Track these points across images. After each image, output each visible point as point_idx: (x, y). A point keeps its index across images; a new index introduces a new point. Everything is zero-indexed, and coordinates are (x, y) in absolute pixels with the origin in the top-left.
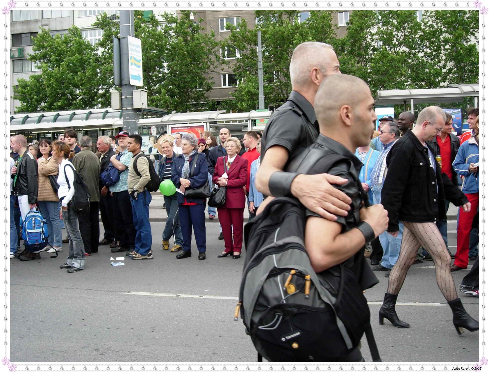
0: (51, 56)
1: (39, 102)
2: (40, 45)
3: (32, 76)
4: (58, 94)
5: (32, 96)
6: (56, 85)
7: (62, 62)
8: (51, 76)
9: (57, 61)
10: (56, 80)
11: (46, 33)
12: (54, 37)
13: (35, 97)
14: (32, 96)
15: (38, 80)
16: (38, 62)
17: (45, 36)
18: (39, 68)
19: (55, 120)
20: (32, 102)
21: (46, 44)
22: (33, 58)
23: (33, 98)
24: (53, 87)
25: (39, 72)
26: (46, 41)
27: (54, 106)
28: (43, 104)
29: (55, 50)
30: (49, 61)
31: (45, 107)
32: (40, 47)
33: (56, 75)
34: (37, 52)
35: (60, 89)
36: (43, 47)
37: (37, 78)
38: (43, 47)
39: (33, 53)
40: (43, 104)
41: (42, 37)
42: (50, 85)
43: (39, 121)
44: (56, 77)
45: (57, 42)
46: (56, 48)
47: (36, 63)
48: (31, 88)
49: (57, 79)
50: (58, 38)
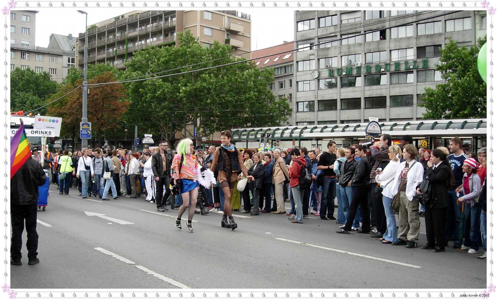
0: (457, 67)
2: (447, 56)
3: (439, 86)
4: (464, 102)
5: (438, 103)
7: (468, 72)
8: (459, 86)
9: (463, 71)
11: (455, 44)
12: (459, 48)
13: (441, 104)
14: (438, 103)
15: (444, 89)
16: (444, 72)
18: (446, 78)
19: (463, 127)
21: (453, 56)
22: (440, 68)
23: (438, 105)
24: (459, 96)
25: (444, 82)
26: (452, 53)
28: (447, 112)
30: (454, 71)
31: (450, 114)
32: (447, 58)
33: (463, 84)
34: (443, 63)
36: (450, 58)
37: (443, 87)
38: (450, 58)
39: (440, 63)
40: (447, 112)
41: (449, 49)
42: (457, 93)
43: (447, 127)
45: (464, 53)
46: (463, 60)
47: (442, 73)
48: (438, 96)
49: (463, 88)
50: (464, 49)
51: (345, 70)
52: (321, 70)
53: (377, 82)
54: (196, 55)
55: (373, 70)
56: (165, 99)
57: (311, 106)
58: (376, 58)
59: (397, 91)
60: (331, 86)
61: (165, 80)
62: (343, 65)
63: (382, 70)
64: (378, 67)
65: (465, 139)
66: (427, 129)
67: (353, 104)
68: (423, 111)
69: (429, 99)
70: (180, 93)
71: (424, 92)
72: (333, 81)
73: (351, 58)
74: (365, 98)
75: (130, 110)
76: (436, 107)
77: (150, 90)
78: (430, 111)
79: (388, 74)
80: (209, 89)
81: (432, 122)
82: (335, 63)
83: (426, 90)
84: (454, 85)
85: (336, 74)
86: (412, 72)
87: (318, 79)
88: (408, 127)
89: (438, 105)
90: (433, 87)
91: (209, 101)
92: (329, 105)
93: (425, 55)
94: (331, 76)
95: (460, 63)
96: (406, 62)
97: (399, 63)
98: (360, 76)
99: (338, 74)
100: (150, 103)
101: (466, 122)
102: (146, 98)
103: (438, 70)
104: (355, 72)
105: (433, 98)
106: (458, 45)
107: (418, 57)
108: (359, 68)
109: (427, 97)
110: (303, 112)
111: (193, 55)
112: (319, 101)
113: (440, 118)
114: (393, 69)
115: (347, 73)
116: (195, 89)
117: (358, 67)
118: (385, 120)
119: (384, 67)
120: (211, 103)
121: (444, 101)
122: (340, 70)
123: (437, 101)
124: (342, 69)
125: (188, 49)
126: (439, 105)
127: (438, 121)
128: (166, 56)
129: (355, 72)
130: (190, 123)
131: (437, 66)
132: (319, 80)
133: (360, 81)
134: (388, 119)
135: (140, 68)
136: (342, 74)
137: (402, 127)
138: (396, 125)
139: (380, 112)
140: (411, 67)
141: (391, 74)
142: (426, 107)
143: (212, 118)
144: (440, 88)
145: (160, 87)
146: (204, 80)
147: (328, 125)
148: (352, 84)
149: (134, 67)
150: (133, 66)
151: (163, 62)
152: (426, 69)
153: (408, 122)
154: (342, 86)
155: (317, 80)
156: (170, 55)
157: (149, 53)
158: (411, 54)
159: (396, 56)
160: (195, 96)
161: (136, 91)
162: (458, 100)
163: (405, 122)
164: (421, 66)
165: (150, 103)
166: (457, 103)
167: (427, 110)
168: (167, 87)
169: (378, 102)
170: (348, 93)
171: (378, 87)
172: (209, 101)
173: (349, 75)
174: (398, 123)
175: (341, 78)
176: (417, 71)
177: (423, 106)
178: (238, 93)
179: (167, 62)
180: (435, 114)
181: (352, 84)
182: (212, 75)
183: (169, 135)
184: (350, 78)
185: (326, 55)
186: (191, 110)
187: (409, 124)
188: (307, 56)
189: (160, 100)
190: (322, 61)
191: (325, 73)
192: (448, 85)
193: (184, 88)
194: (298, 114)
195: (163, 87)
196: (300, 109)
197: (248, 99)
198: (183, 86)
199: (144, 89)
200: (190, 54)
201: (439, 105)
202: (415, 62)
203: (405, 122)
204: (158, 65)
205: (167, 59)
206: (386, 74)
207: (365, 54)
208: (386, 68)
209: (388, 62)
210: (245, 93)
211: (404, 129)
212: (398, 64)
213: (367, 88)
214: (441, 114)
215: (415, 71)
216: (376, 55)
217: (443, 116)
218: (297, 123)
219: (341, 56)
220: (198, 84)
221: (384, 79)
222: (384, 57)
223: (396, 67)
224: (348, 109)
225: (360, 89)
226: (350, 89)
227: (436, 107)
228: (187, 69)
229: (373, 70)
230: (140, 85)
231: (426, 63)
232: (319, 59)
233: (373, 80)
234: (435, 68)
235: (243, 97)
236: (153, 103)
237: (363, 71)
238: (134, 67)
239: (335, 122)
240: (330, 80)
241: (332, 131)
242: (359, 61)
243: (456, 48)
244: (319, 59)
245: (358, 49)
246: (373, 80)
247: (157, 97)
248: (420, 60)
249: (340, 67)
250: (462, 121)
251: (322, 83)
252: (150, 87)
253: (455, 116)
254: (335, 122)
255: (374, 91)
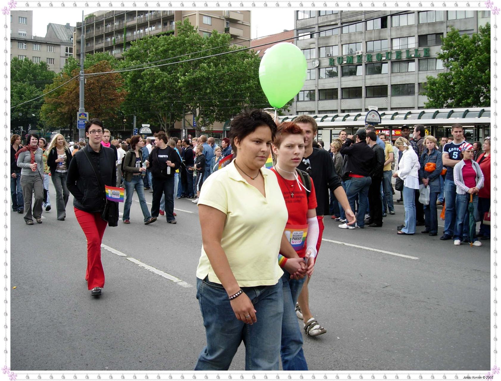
0: (459, 55)
1: (446, 98)
3: (441, 75)
4: (466, 91)
5: (440, 92)
6: (465, 83)
8: (461, 74)
9: (465, 60)
10: (466, 78)
11: (457, 32)
12: (461, 37)
13: (443, 93)
14: (440, 92)
15: (446, 78)
16: (446, 60)
17: (454, 36)
18: (448, 67)
20: (439, 98)
21: (454, 44)
22: (442, 57)
23: (440, 94)
24: (461, 84)
25: (445, 70)
26: (454, 41)
27: (462, 103)
28: (449, 101)
29: (463, 48)
30: (456, 60)
31: (452, 103)
32: (449, 47)
33: (466, 72)
34: (445, 51)
35: (468, 87)
36: (451, 46)
37: (445, 75)
38: (451, 46)
39: (442, 52)
40: (449, 101)
41: (451, 37)
42: (459, 82)
43: (449, 116)
44: (466, 75)
45: (466, 42)
46: (465, 48)
47: (444, 61)
50: (466, 37)
51: (346, 59)
52: (321, 59)
53: (379, 71)
54: (195, 44)
55: (375, 59)
56: (164, 89)
57: (311, 95)
58: (376, 47)
59: (398, 80)
60: (332, 74)
61: (163, 69)
62: (344, 54)
63: (384, 58)
64: (379, 56)
65: (467, 128)
66: (429, 118)
67: (354, 93)
68: (425, 100)
69: (430, 88)
70: (178, 82)
71: (426, 81)
72: (334, 70)
73: (352, 46)
74: (366, 87)
75: (128, 99)
76: (438, 95)
77: (148, 80)
78: (432, 100)
79: (389, 62)
80: (208, 79)
81: (434, 110)
82: (336, 52)
83: (428, 79)
84: (456, 74)
85: (336, 63)
86: (413, 61)
87: (319, 68)
88: (409, 116)
89: (440, 94)
90: (435, 76)
91: (208, 91)
92: (330, 94)
93: (427, 43)
94: (332, 64)
95: (462, 52)
96: (408, 51)
97: (400, 51)
98: (361, 65)
99: (339, 62)
100: (149, 93)
101: (468, 111)
102: (144, 88)
103: (440, 58)
104: (356, 61)
105: (435, 87)
106: (460, 33)
107: (420, 45)
108: (360, 57)
109: (429, 85)
110: (304, 101)
111: (192, 44)
112: (319, 90)
113: (442, 107)
114: (394, 57)
115: (347, 61)
116: (194, 79)
117: (359, 56)
118: (386, 109)
119: (386, 55)
120: (210, 93)
121: (446, 89)
122: (340, 59)
123: (439, 90)
124: (342, 58)
125: (187, 39)
126: (440, 94)
127: (440, 110)
128: (164, 45)
129: (356, 61)
130: (189, 113)
131: (439, 54)
132: (319, 69)
133: (361, 70)
134: (389, 108)
135: (138, 58)
136: (342, 62)
137: (404, 116)
138: (397, 114)
139: (381, 102)
140: (413, 56)
141: (392, 63)
142: (428, 96)
143: (211, 108)
144: (442, 77)
145: (159, 76)
146: (204, 69)
147: (328, 115)
148: (353, 73)
149: (132, 56)
150: (130, 55)
151: (161, 51)
152: (428, 57)
153: (409, 111)
154: (343, 75)
155: (317, 69)
156: (168, 44)
157: (146, 42)
158: (413, 43)
159: (397, 45)
160: (194, 85)
161: (134, 80)
162: (461, 89)
163: (406, 111)
164: (422, 54)
165: (149, 93)
166: (458, 91)
167: (428, 99)
168: (166, 77)
169: (379, 91)
170: (349, 82)
171: (380, 75)
172: (208, 91)
173: (350, 63)
174: (399, 112)
175: (342, 67)
176: (419, 60)
177: (424, 94)
178: (237, 83)
179: (166, 51)
180: (437, 102)
181: (353, 73)
182: (212, 64)
183: (168, 125)
184: (350, 67)
185: (327, 44)
186: (191, 100)
187: (410, 113)
188: (307, 44)
189: (159, 89)
190: (323, 50)
191: (326, 62)
192: (450, 74)
193: (182, 78)
194: (299, 103)
195: (162, 76)
196: (301, 98)
197: (248, 88)
198: (181, 75)
199: (142, 79)
200: (188, 43)
201: (440, 94)
202: (417, 50)
203: (406, 111)
204: (157, 54)
205: (165, 48)
206: (387, 63)
207: (366, 42)
208: (387, 57)
209: (389, 51)
210: (244, 82)
211: (406, 118)
212: (399, 53)
213: (369, 76)
214: (444, 103)
215: (416, 60)
216: (377, 43)
217: (445, 105)
218: (297, 112)
219: (342, 45)
220: (197, 74)
221: (386, 68)
222: (385, 45)
223: (397, 56)
224: (349, 98)
225: (361, 78)
226: (351, 78)
227: (438, 95)
228: (186, 58)
229: (375, 59)
230: (138, 75)
231: (427, 51)
232: (319, 48)
233: (374, 68)
234: (437, 56)
235: (243, 86)
236: (152, 93)
237: (364, 60)
238: (132, 56)
239: (336, 111)
240: (331, 69)
241: (333, 120)
242: (361, 50)
243: (458, 35)
244: (319, 48)
245: (360, 38)
246: (374, 68)
247: (156, 87)
248: (421, 49)
249: (340, 55)
250: (464, 110)
251: (323, 72)
252: (148, 77)
253: (458, 105)
254: (336, 111)
255: (375, 80)
